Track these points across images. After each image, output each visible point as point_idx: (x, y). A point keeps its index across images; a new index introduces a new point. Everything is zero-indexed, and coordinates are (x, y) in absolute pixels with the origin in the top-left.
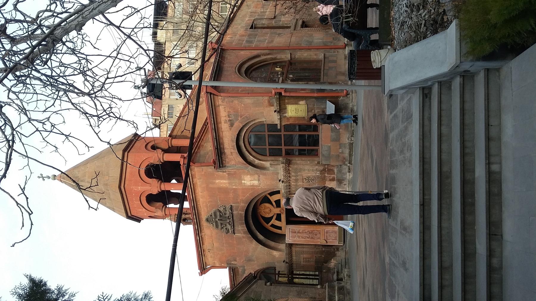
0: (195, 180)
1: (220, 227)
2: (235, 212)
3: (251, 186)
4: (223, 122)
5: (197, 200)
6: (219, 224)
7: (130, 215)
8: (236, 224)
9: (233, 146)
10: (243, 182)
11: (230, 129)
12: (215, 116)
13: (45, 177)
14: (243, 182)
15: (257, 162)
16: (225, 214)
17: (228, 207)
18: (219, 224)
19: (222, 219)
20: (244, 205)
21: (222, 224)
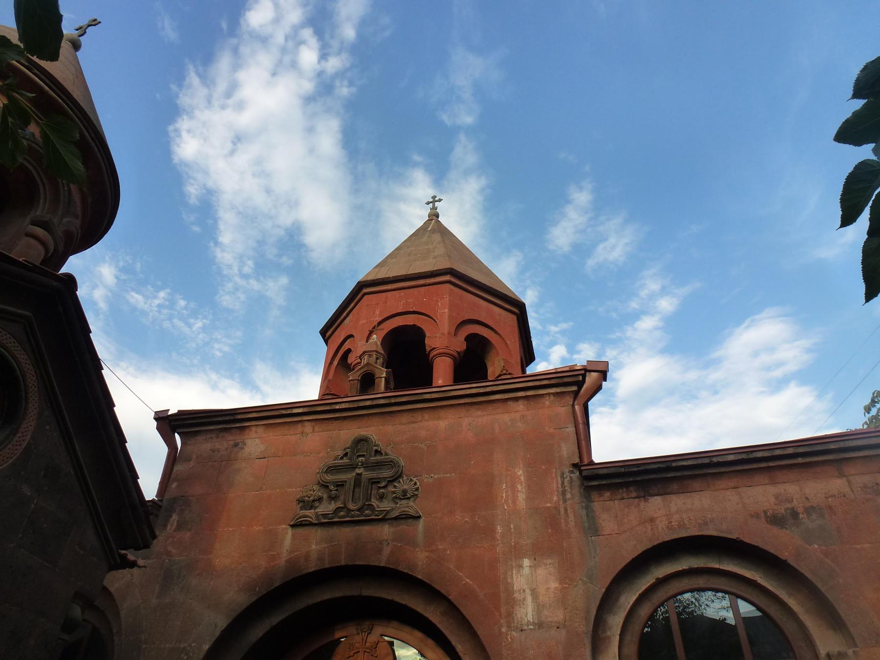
0: (520, 406)
1: (329, 478)
2: (386, 531)
3: (510, 592)
4: (780, 489)
5: (442, 413)
6: (342, 477)
7: (365, 290)
8: (335, 531)
9: (681, 525)
10: (526, 562)
11: (756, 515)
12: (800, 460)
13: (434, 205)
14: (526, 562)
15: (616, 621)
16: (381, 497)
17: (410, 506)
18: (342, 477)
19: (363, 484)
20: (419, 561)
21: (340, 485)
